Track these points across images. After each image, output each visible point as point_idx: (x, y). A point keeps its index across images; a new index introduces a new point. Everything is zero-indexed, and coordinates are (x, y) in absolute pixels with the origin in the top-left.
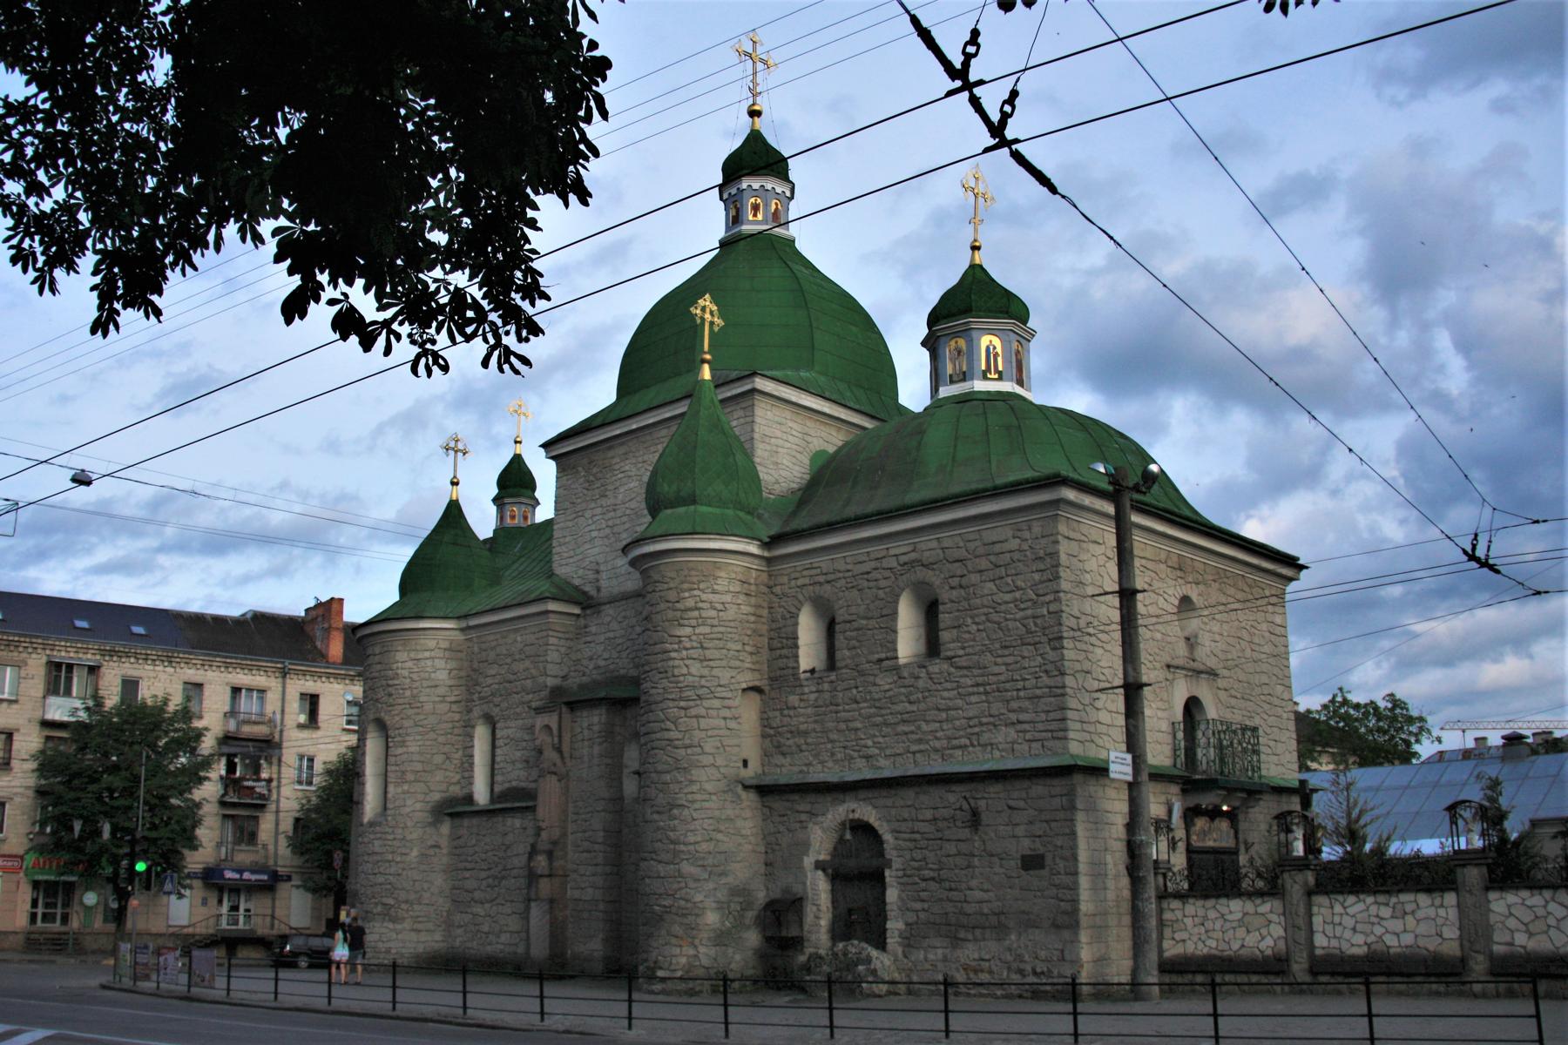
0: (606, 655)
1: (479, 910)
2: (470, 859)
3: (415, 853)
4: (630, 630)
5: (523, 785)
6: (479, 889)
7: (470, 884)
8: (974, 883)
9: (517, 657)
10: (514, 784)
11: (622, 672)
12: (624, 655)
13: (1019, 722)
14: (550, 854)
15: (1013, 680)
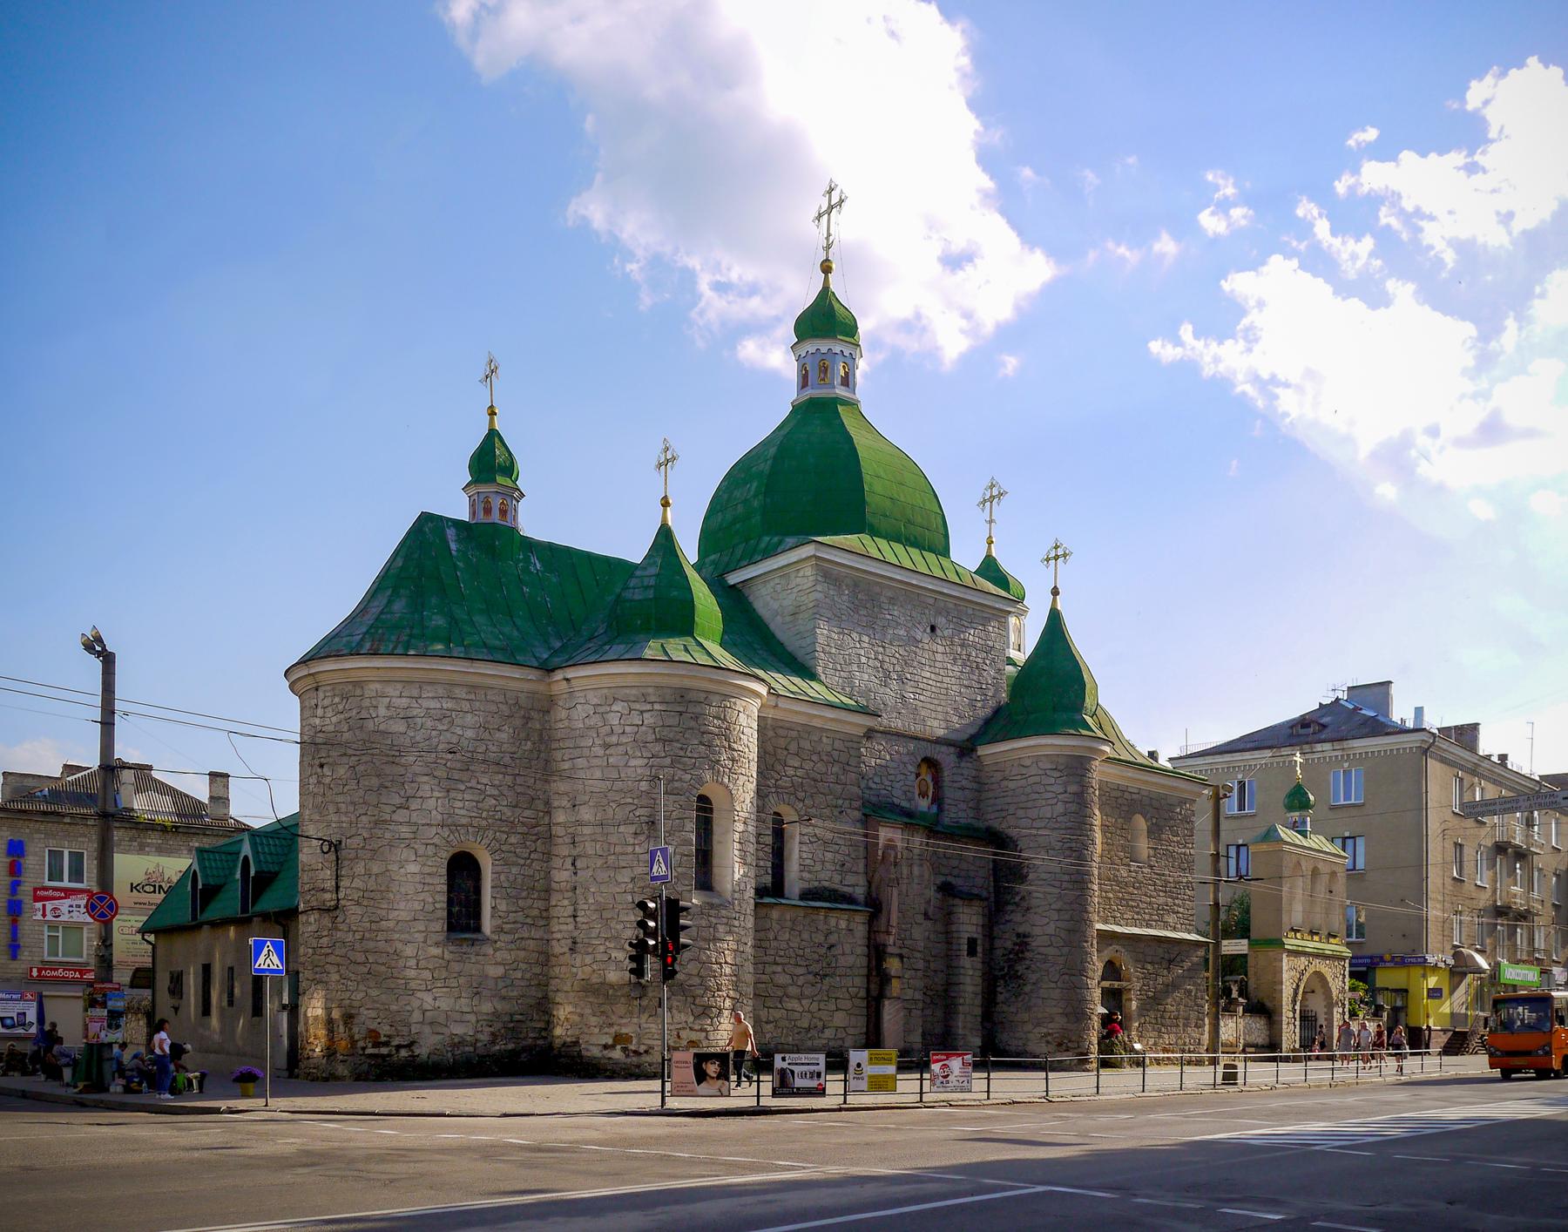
0: (877, 779)
1: (794, 1004)
2: (782, 953)
3: (749, 944)
4: (902, 766)
5: (836, 887)
6: (794, 984)
7: (782, 979)
8: (1169, 1000)
9: (825, 758)
10: (826, 884)
11: (895, 800)
12: (897, 785)
13: (1178, 912)
14: (901, 957)
15: (1176, 888)
